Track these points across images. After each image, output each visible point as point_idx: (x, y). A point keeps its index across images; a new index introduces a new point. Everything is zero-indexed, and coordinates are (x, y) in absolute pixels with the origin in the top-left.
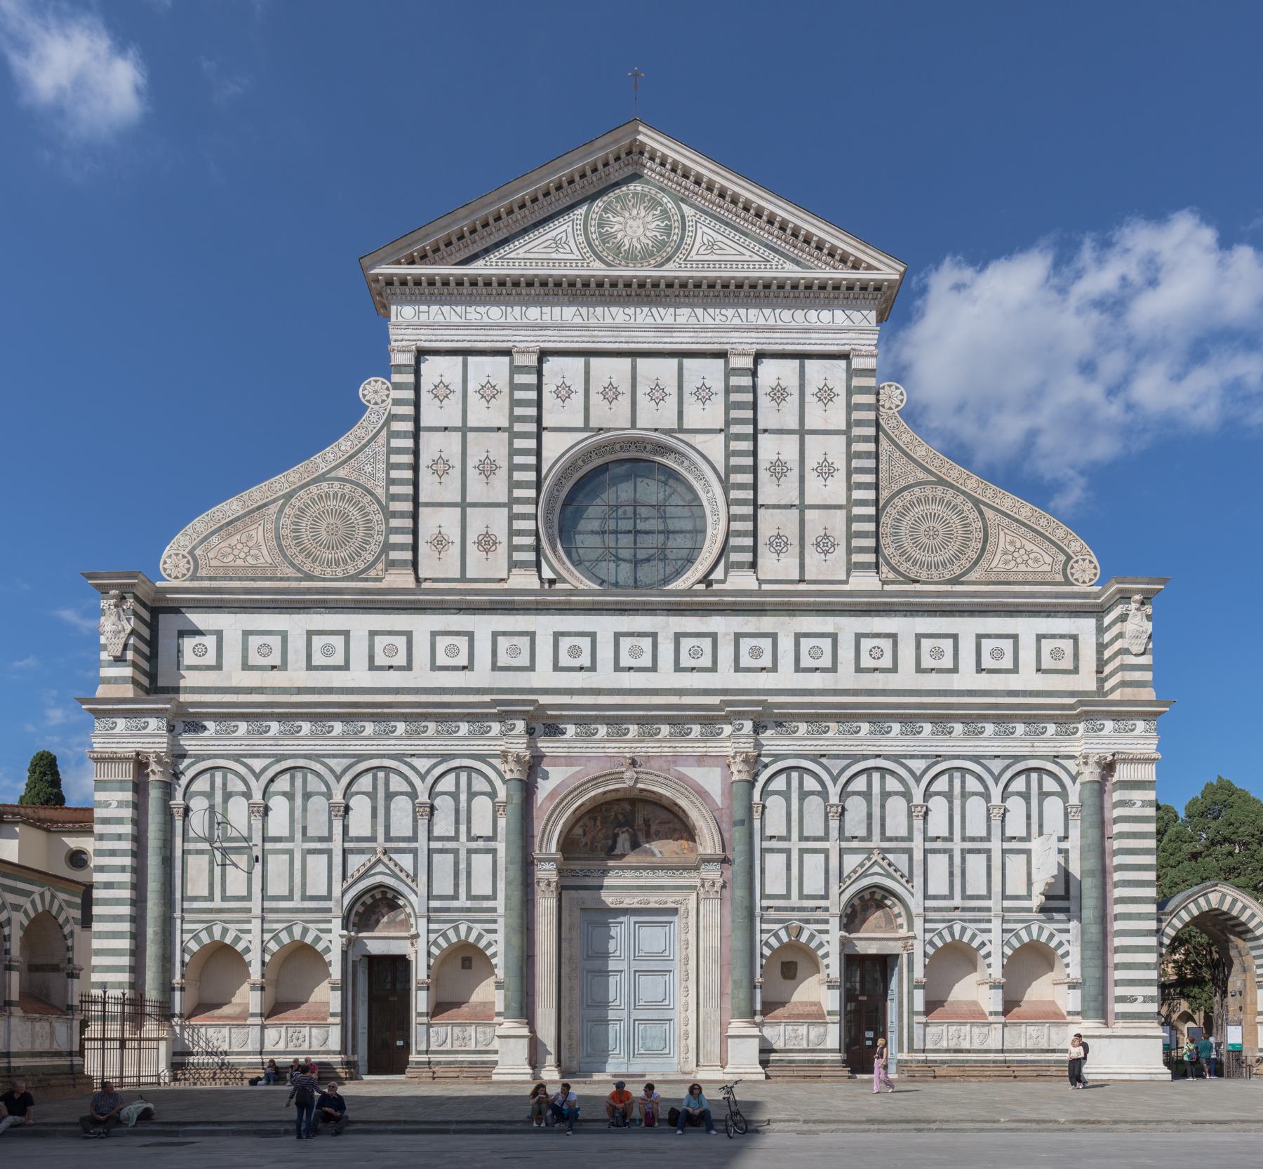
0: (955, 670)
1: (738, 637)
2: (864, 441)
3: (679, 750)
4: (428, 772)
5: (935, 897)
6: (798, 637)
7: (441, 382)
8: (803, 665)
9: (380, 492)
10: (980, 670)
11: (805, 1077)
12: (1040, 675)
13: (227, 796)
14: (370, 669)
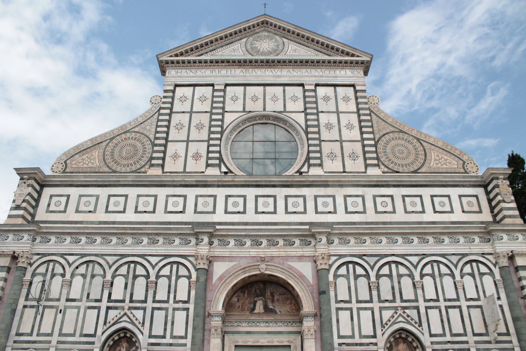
0: (423, 212)
1: (316, 197)
3: (289, 253)
4: (156, 264)
5: (435, 335)
6: (345, 197)
7: (184, 96)
8: (349, 210)
9: (152, 137)
12: (464, 214)
14: (135, 212)
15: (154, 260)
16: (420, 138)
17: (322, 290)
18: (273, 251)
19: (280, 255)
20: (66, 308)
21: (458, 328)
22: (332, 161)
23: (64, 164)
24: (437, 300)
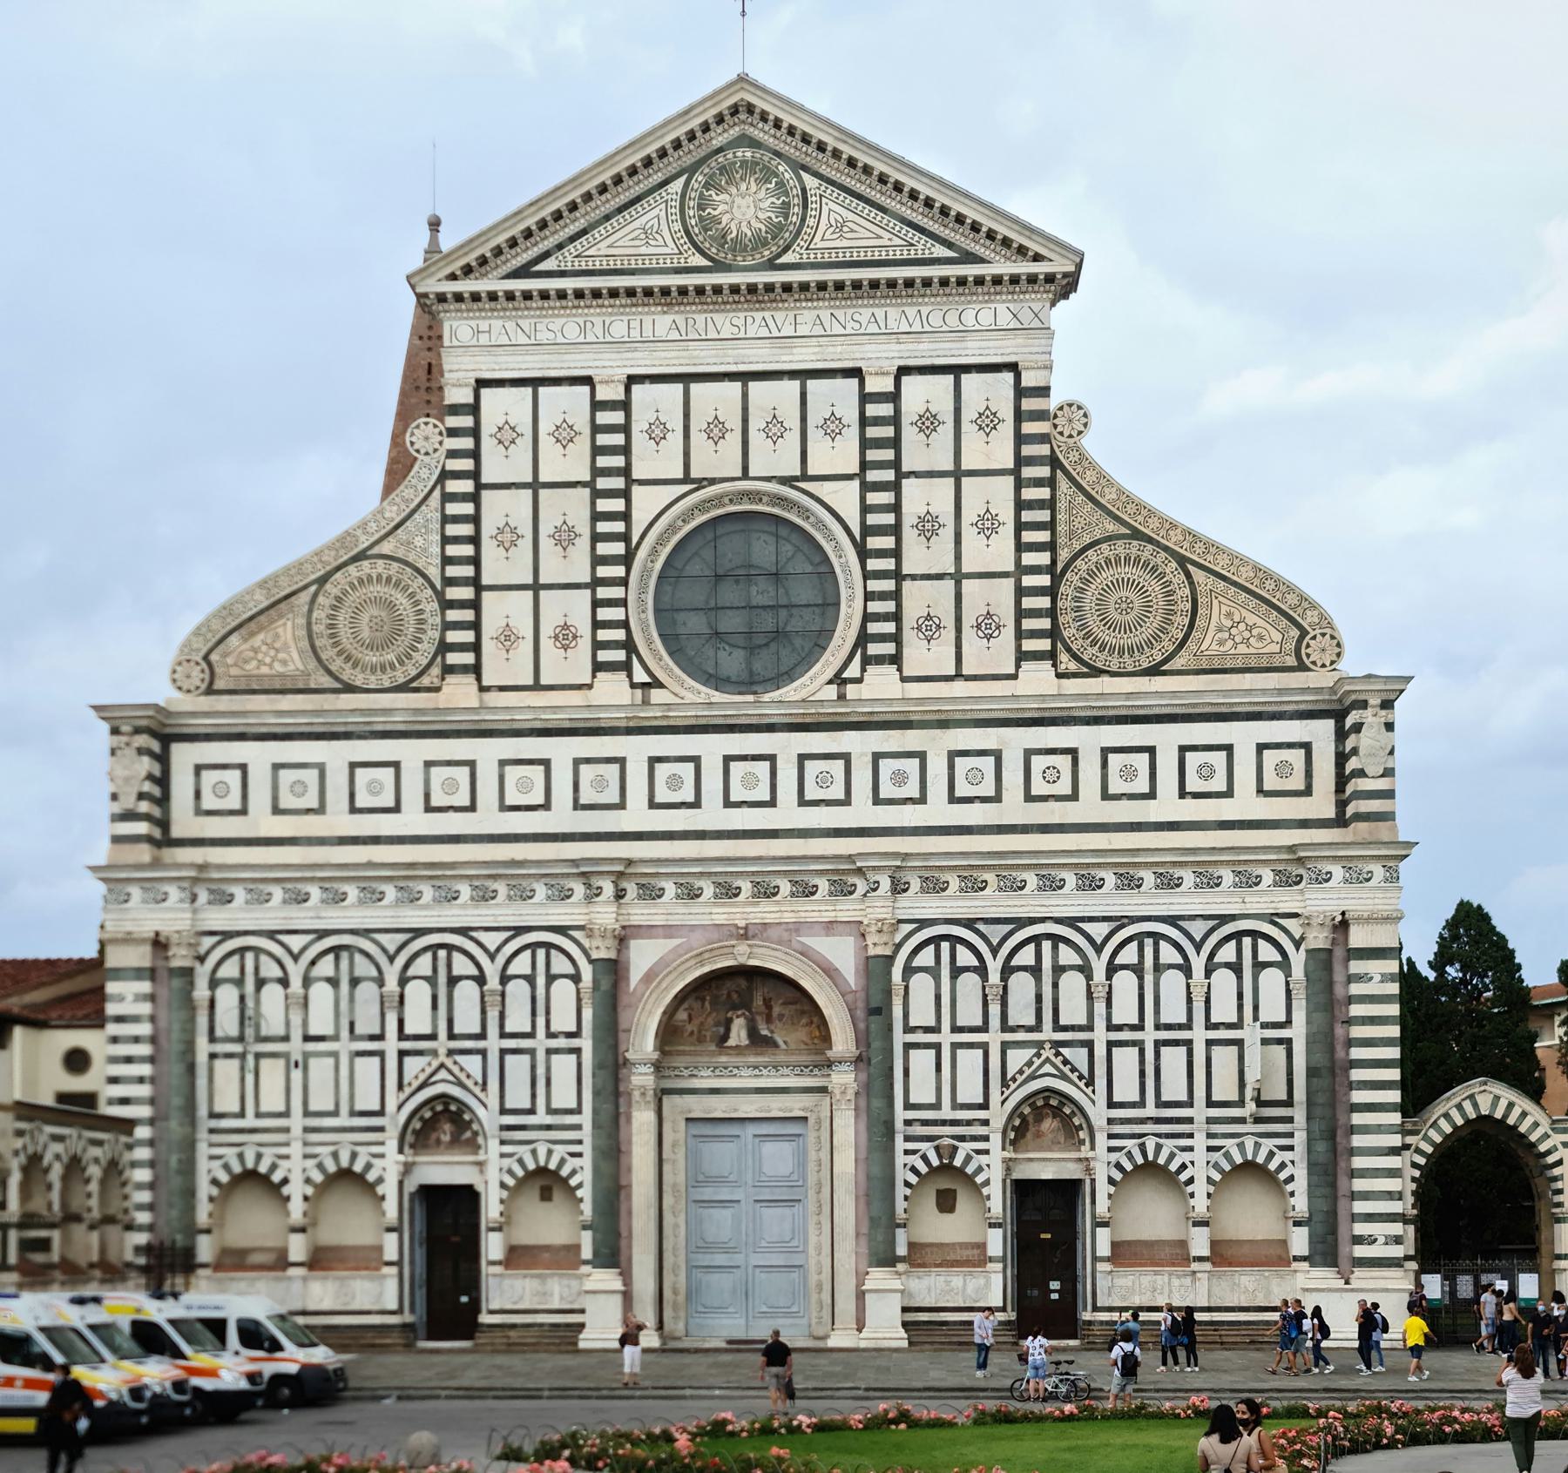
1: (877, 757)
2: (1035, 486)
3: (803, 914)
4: (498, 950)
5: (1122, 1105)
6: (953, 755)
8: (958, 794)
9: (434, 573)
10: (1183, 794)
11: (960, 1343)
12: (1263, 800)
13: (260, 983)
15: (491, 941)
16: (1188, 554)
17: (874, 1004)
18: (766, 912)
20: (307, 1056)
21: (1174, 1088)
23: (204, 665)
24: (1140, 1027)
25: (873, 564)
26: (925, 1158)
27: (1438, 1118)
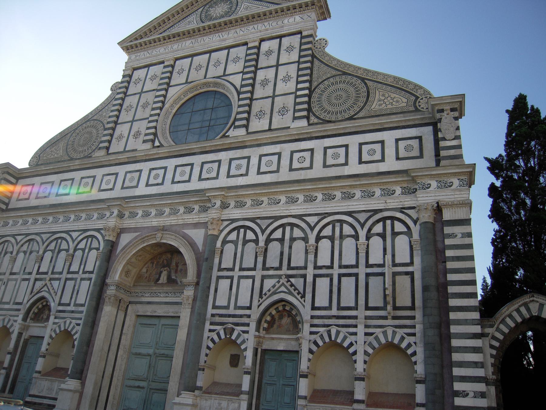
0: (346, 164)
3: (186, 220)
5: (319, 308)
9: (105, 122)
19: (178, 223)
20: (9, 280)
21: (348, 300)
22: (260, 119)
24: (331, 267)
25: (242, 96)
26: (218, 335)
27: (505, 318)
